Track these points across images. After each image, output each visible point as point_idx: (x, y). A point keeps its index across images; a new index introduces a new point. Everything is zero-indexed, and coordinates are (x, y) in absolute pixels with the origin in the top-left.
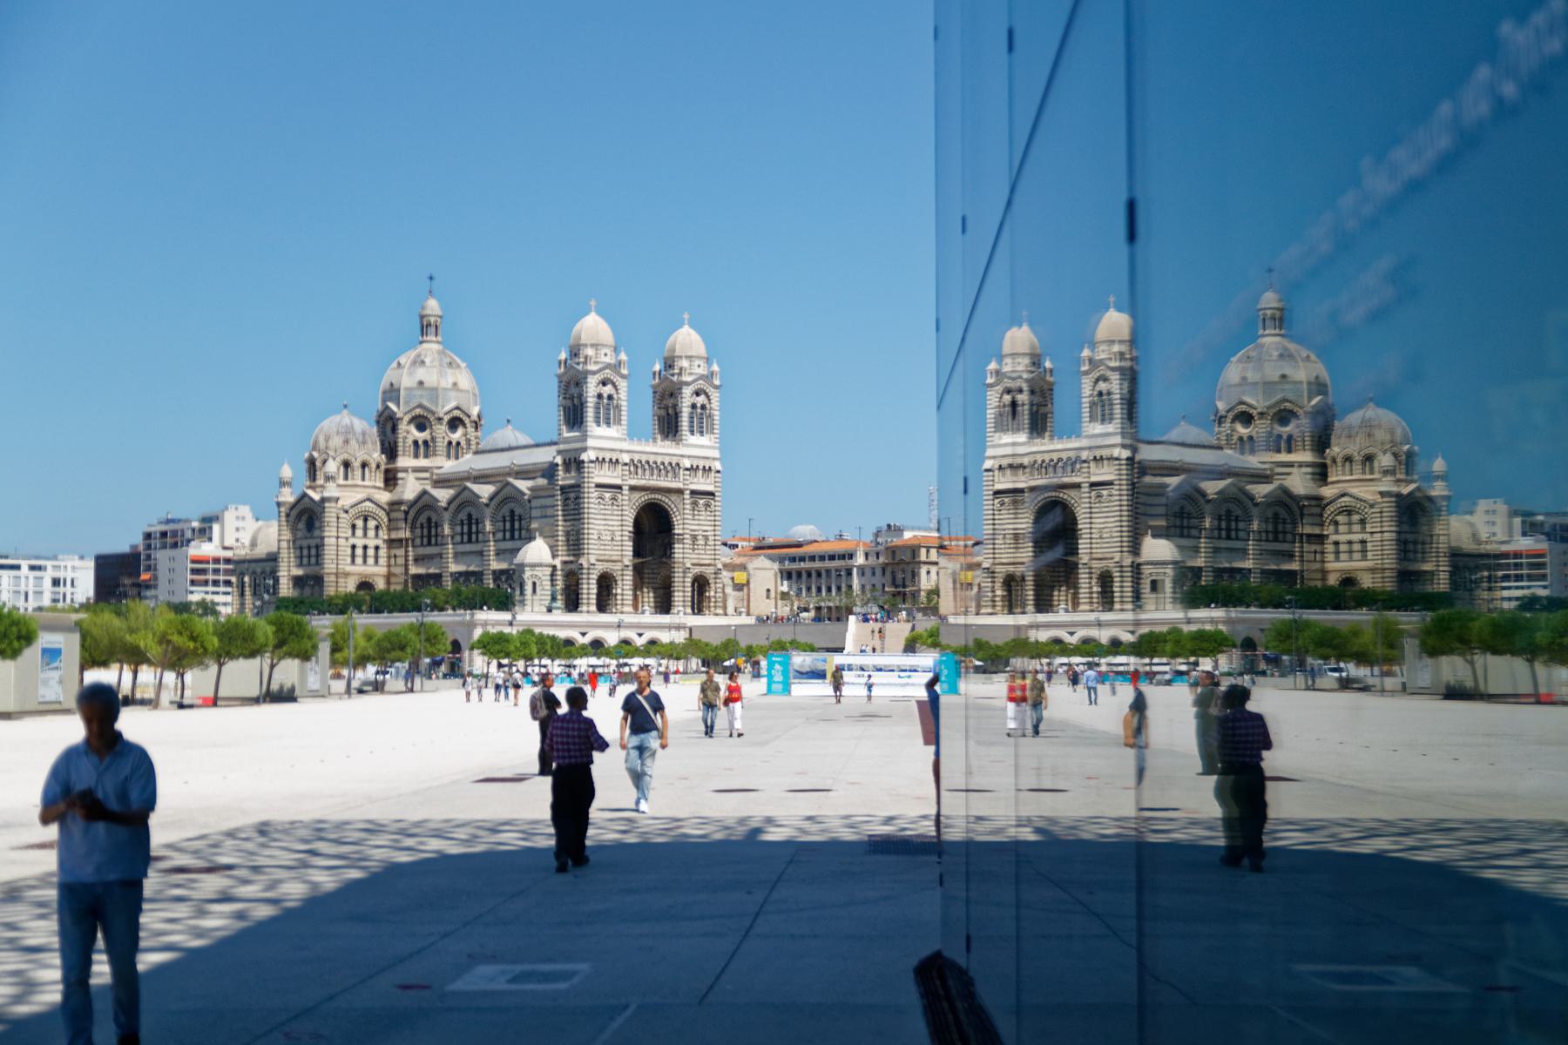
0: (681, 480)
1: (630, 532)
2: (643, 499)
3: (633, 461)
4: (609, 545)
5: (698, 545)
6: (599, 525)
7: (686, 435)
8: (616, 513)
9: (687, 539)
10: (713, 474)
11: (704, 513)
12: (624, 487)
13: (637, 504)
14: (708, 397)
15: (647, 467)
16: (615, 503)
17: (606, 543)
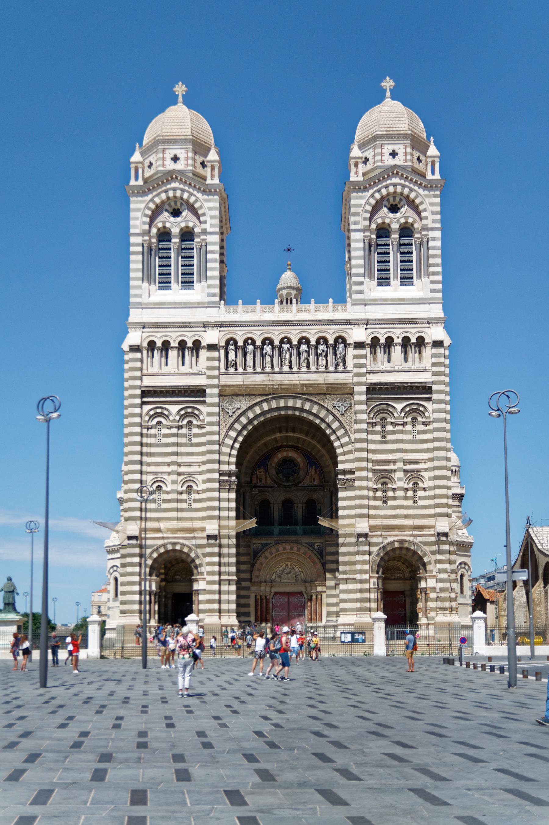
0: (349, 368)
1: (221, 474)
2: (258, 410)
3: (236, 343)
4: (178, 501)
5: (394, 490)
6: (157, 464)
7: (362, 283)
8: (195, 440)
9: (361, 479)
10: (428, 351)
11: (409, 427)
12: (208, 391)
13: (244, 420)
14: (415, 208)
15: (268, 349)
16: (195, 422)
17: (174, 496)
